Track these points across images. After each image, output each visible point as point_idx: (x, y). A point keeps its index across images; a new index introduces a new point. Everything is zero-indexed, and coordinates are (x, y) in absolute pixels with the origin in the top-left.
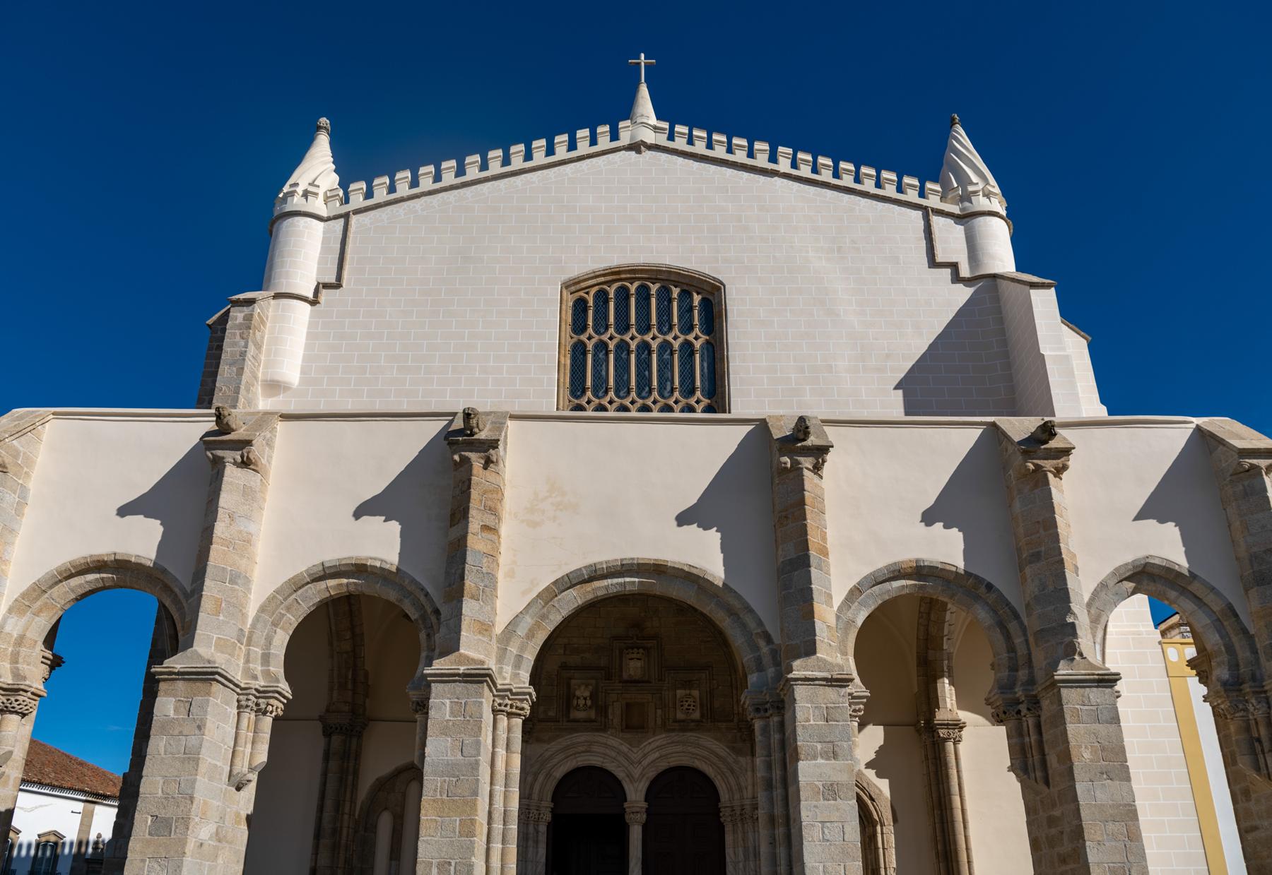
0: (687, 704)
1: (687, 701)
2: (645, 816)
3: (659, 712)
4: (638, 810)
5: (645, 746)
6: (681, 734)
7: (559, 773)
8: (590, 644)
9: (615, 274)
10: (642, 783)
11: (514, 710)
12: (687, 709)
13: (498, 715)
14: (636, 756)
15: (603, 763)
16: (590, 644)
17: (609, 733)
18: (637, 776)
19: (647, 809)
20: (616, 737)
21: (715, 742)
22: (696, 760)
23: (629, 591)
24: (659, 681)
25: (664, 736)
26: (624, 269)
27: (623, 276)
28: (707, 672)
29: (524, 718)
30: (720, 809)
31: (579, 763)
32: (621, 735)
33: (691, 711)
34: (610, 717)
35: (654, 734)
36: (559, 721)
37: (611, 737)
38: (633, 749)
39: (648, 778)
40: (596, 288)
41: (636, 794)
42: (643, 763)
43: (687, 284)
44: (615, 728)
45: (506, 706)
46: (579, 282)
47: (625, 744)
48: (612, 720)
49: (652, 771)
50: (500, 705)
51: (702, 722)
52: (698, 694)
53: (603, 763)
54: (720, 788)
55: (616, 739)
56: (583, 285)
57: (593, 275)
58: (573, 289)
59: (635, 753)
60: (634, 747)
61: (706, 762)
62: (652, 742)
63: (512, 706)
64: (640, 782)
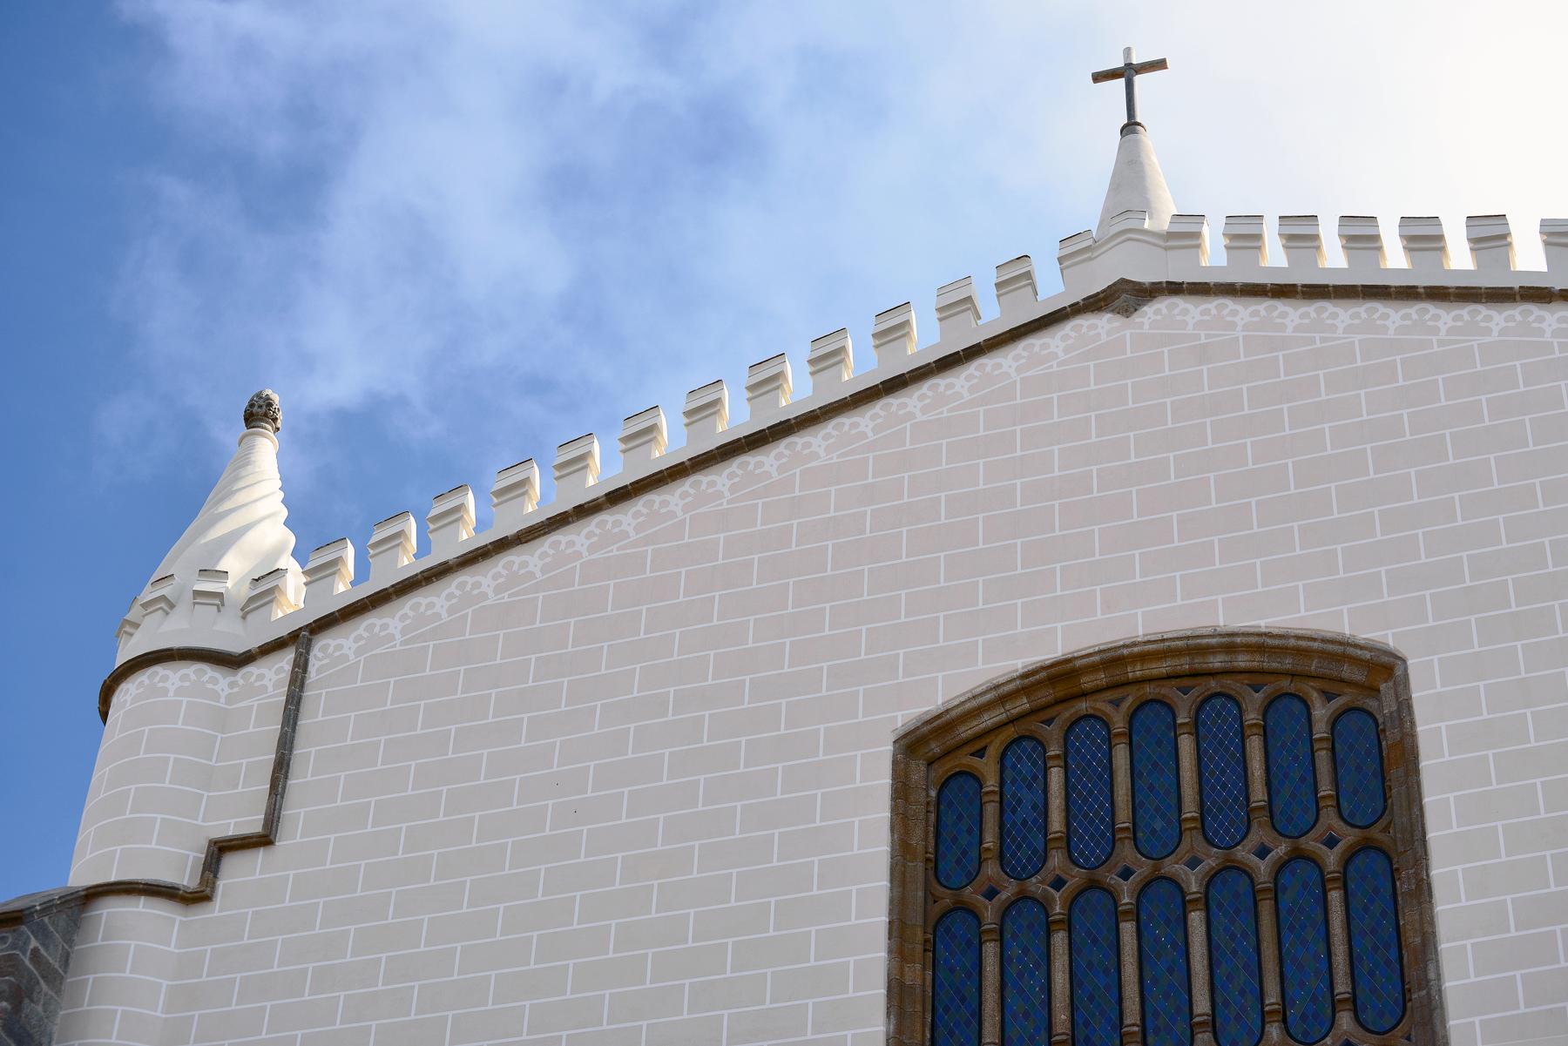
27: (1087, 682)
40: (1011, 732)
43: (1293, 675)
56: (965, 731)
58: (935, 748)
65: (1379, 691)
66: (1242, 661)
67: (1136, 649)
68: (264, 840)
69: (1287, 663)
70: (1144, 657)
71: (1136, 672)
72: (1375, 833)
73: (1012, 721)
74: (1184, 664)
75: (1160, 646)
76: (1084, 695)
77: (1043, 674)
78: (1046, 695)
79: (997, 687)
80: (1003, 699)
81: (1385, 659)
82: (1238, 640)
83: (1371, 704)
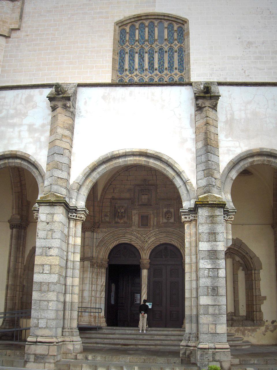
1: (168, 214)
2: (149, 265)
3: (156, 219)
7: (111, 247)
9: (139, 18)
11: (77, 218)
13: (70, 220)
15: (130, 242)
19: (150, 262)
22: (172, 241)
23: (130, 164)
24: (155, 204)
25: (157, 229)
26: (143, 15)
27: (143, 18)
28: (177, 200)
29: (82, 221)
33: (170, 218)
36: (111, 223)
41: (145, 256)
45: (74, 216)
46: (123, 22)
50: (71, 216)
51: (175, 223)
52: (173, 211)
57: (129, 18)
58: (120, 25)
63: (76, 216)
65: (184, 25)
66: (166, 18)
67: (150, 14)
68: (19, 29)
69: (172, 19)
70: (151, 15)
71: (149, 17)
72: (182, 45)
73: (131, 22)
74: (157, 17)
75: (154, 14)
76: (142, 20)
77: (136, 16)
78: (136, 19)
79: (130, 17)
80: (130, 19)
81: (186, 20)
82: (166, 15)
83: (183, 26)
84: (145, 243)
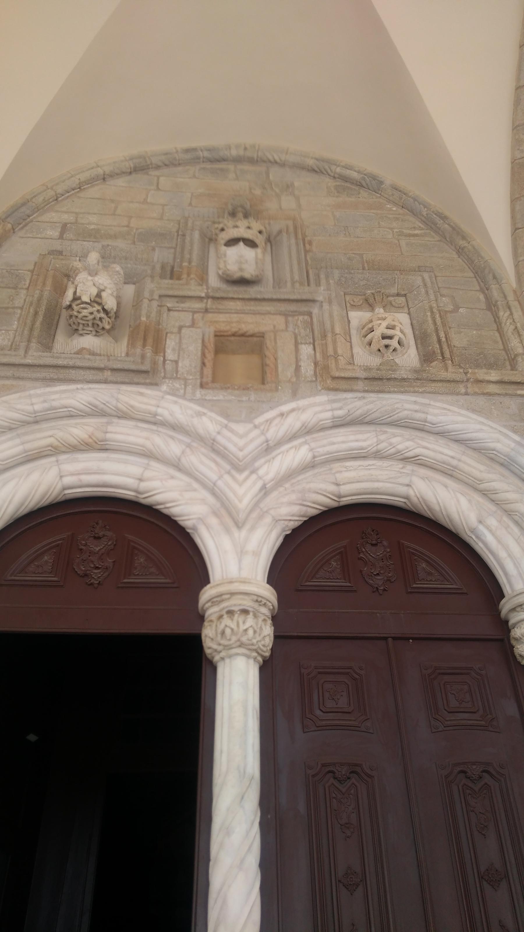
0: (384, 324)
3: (306, 350)
4: (247, 603)
5: (270, 421)
6: (372, 396)
8: (128, 226)
10: (259, 533)
12: (384, 337)
14: (241, 443)
16: (128, 226)
17: (164, 388)
18: (246, 501)
20: (183, 397)
21: (474, 416)
22: (415, 479)
25: (322, 398)
30: (507, 622)
31: (68, 480)
32: (199, 393)
34: (170, 355)
35: (295, 395)
37: (168, 397)
38: (233, 426)
39: (276, 521)
42: (261, 472)
44: (185, 380)
47: (210, 414)
48: (176, 362)
49: (291, 503)
53: (141, 480)
54: (502, 554)
55: (181, 401)
59: (241, 437)
60: (237, 422)
61: (446, 487)
62: (293, 410)
64: (253, 528)
84: (241, 477)
